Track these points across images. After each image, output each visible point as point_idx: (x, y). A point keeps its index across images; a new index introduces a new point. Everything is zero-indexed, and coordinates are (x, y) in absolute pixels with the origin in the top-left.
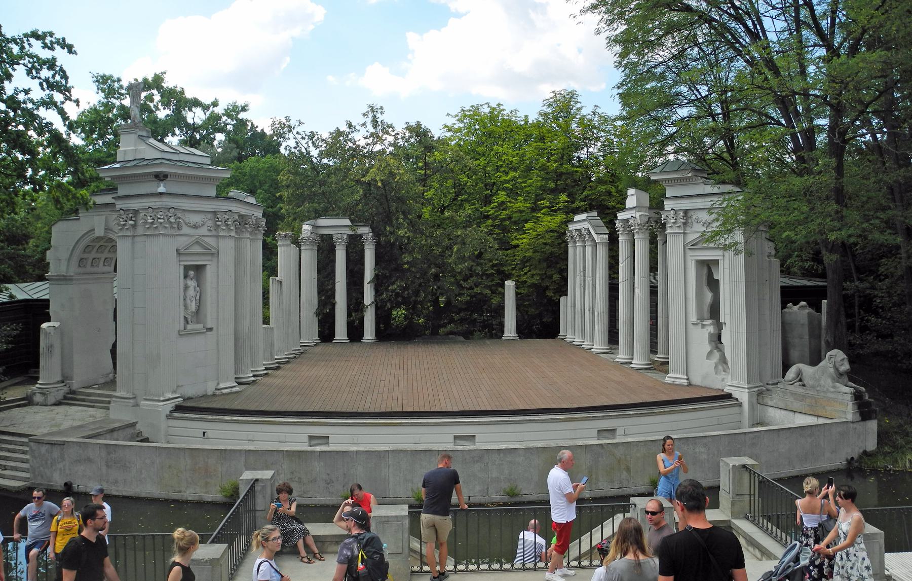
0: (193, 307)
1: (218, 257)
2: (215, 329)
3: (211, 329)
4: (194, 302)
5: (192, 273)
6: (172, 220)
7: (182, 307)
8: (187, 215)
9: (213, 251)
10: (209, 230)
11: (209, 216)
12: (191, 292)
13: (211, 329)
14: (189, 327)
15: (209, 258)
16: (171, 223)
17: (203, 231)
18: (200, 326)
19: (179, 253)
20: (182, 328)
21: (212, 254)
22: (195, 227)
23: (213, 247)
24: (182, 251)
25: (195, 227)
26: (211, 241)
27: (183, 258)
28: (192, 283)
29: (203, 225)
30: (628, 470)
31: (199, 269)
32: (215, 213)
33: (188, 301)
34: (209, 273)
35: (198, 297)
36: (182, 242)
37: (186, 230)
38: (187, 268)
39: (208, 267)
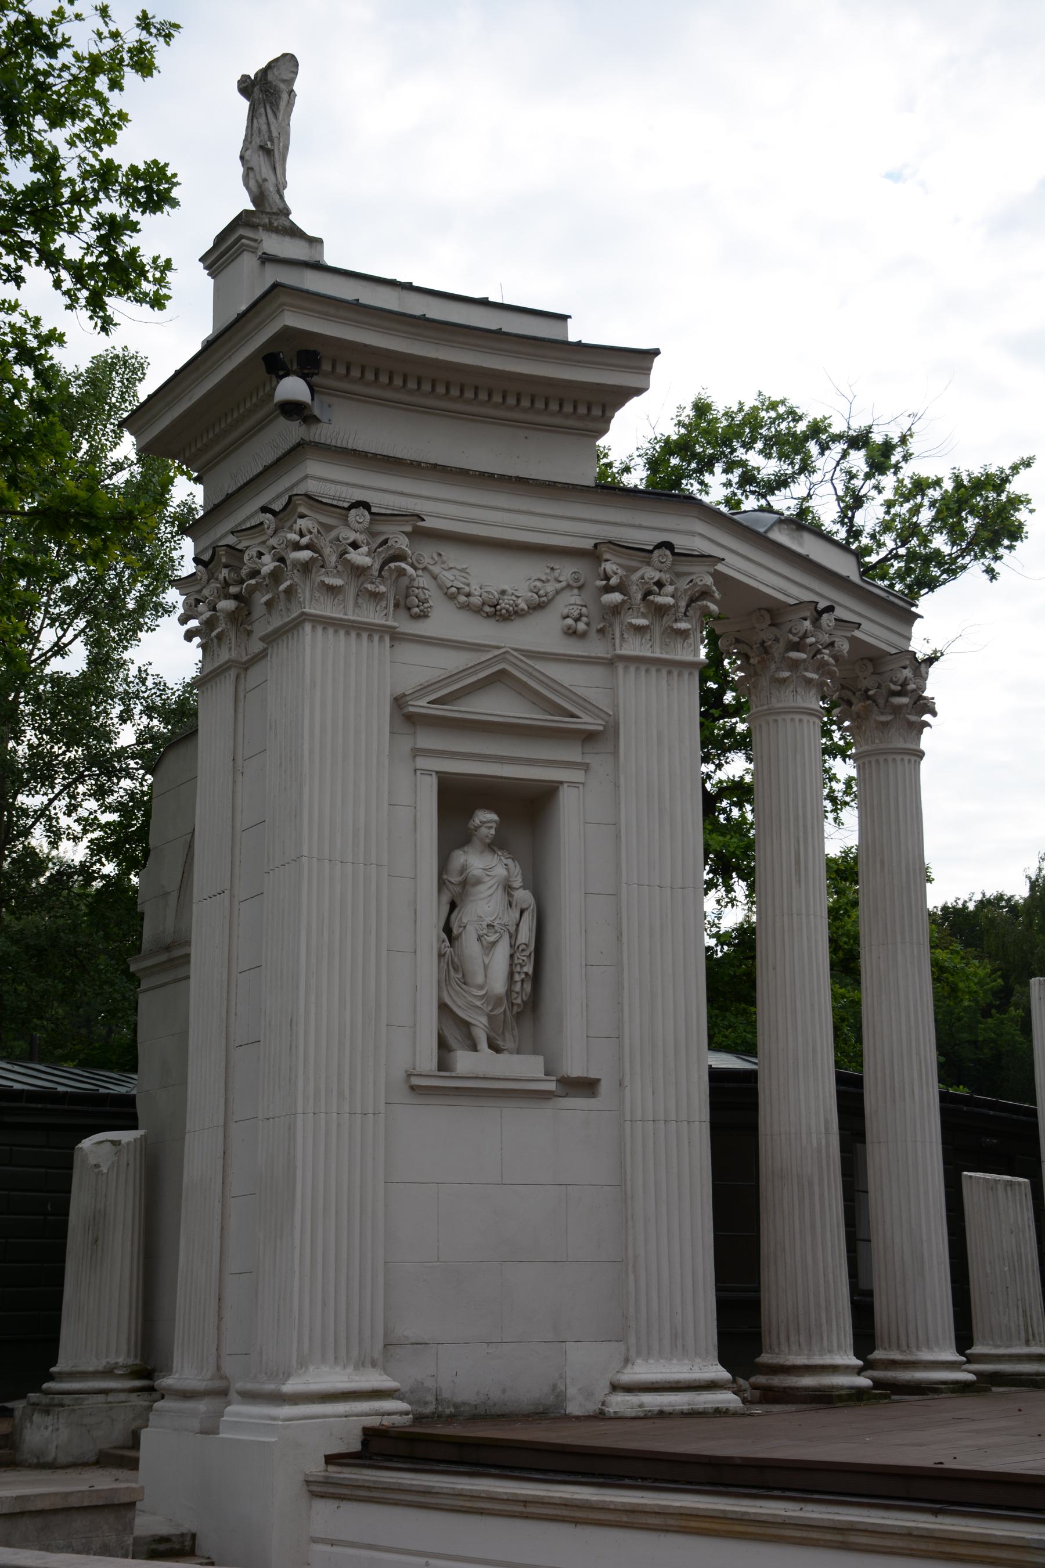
0: (493, 971)
1: (615, 753)
2: (603, 1088)
3: (587, 1086)
4: (502, 952)
5: (486, 819)
6: (359, 557)
7: (428, 968)
8: (455, 557)
9: (588, 722)
10: (571, 633)
11: (567, 570)
12: (485, 907)
14: (464, 1061)
15: (572, 753)
16: (359, 572)
17: (541, 634)
18: (523, 1067)
20: (428, 1060)
21: (588, 737)
22: (497, 612)
23: (586, 704)
24: (421, 705)
25: (497, 612)
27: (427, 740)
29: (538, 607)
31: (527, 811)
32: (593, 555)
33: (470, 946)
34: (573, 818)
35: (526, 935)
38: (458, 800)
39: (567, 799)
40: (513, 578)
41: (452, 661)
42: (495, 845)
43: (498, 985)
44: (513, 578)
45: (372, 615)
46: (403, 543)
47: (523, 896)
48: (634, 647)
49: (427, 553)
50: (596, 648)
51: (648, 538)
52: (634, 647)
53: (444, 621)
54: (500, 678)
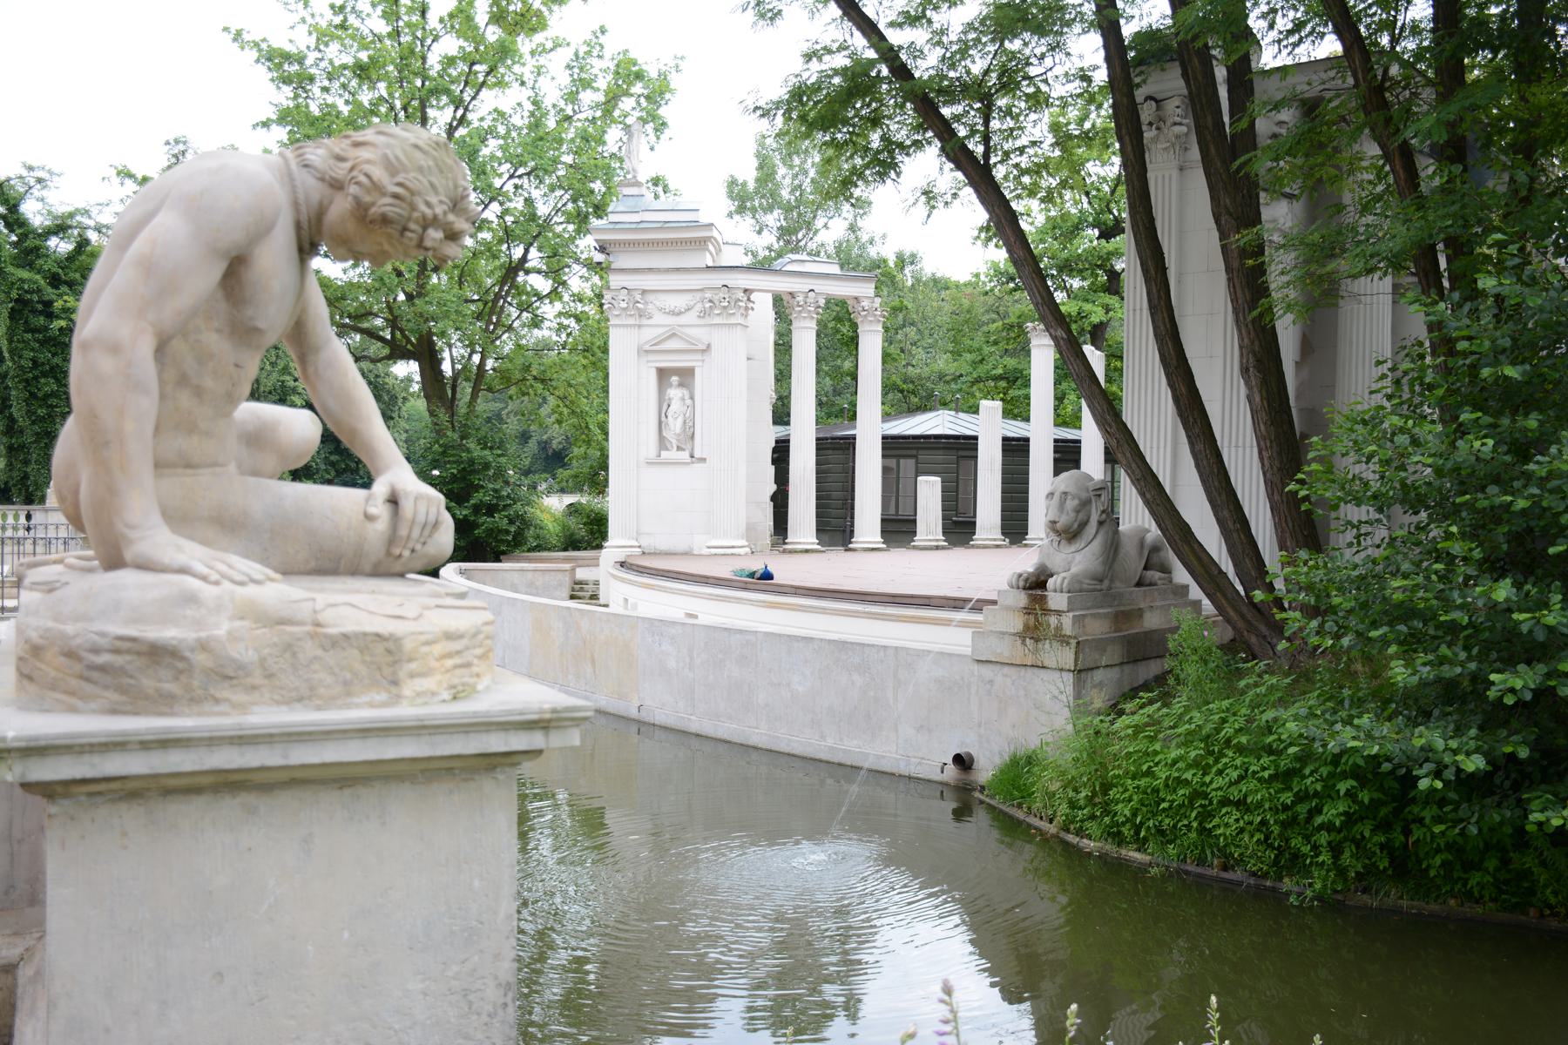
0: (675, 426)
3: (703, 460)
5: (675, 379)
6: (624, 305)
8: (662, 297)
11: (699, 295)
13: (703, 460)
14: (664, 454)
15: (699, 356)
17: (690, 318)
18: (685, 455)
19: (643, 352)
24: (647, 347)
26: (701, 335)
27: (651, 357)
28: (675, 393)
30: (593, 662)
31: (686, 375)
32: (701, 290)
36: (649, 334)
37: (659, 318)
38: (663, 374)
40: (679, 302)
41: (660, 331)
42: (681, 385)
43: (678, 430)
44: (679, 302)
45: (631, 321)
46: (638, 297)
47: (689, 402)
48: (718, 320)
49: (650, 297)
50: (708, 321)
51: (719, 283)
52: (718, 320)
53: (659, 318)
54: (674, 335)
